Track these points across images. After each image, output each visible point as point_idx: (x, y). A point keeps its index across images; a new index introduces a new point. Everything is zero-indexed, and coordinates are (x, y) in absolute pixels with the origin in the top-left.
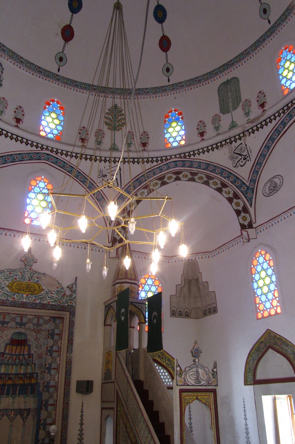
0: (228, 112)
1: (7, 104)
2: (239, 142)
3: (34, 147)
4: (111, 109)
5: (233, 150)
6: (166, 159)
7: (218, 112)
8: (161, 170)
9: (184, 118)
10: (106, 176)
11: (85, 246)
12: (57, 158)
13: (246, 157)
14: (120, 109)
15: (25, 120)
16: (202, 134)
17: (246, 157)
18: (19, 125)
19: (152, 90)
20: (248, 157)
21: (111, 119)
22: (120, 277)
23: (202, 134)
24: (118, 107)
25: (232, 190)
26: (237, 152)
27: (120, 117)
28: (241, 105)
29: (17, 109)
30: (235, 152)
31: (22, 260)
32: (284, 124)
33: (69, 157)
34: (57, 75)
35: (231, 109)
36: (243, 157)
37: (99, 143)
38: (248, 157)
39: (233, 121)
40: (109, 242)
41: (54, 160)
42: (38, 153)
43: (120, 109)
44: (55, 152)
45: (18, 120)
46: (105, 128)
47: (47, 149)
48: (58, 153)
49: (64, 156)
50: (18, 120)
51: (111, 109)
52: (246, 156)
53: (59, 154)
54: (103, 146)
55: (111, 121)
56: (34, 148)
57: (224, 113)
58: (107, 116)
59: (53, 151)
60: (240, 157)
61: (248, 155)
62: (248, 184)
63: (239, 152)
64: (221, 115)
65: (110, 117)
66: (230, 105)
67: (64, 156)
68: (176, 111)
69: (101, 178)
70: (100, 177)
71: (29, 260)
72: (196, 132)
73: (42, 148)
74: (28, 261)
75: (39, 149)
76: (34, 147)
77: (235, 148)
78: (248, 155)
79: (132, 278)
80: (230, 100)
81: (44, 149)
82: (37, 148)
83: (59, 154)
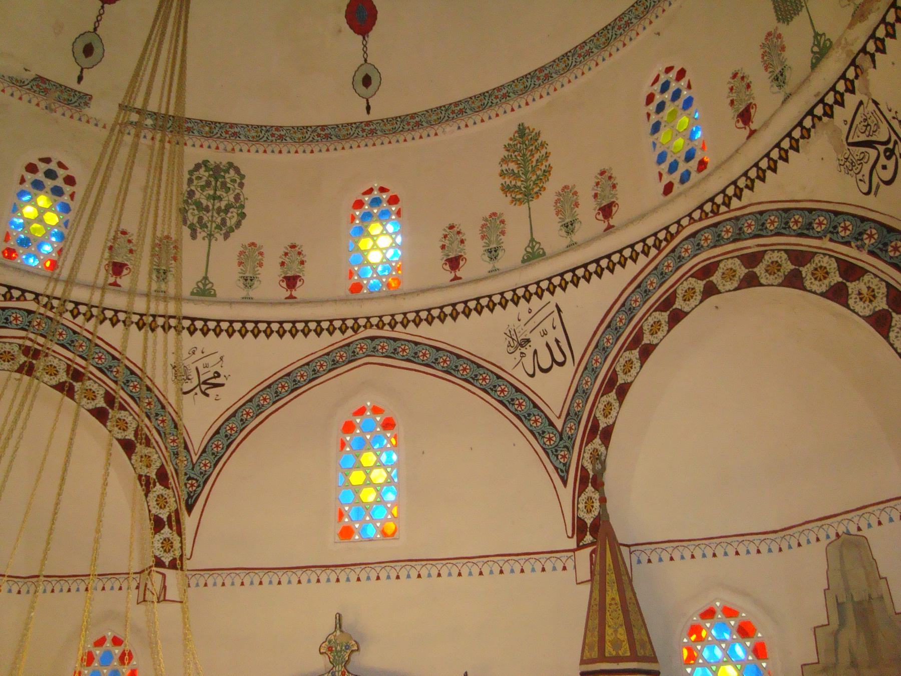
1: (261, 254)
2: (851, 101)
4: (511, 142)
5: (844, 137)
8: (663, 277)
9: (403, 213)
10: (528, 341)
11: (501, 563)
12: (395, 340)
13: (891, 146)
14: (533, 134)
17: (891, 146)
19: (598, 40)
20: (896, 143)
22: (587, 655)
24: (527, 131)
26: (856, 140)
27: (537, 156)
30: (850, 140)
31: (322, 651)
34: (368, 123)
36: (881, 148)
38: (896, 143)
39: (816, 35)
40: (568, 537)
41: (389, 347)
43: (533, 134)
47: (368, 325)
50: (291, 282)
51: (511, 142)
52: (888, 142)
53: (399, 327)
55: (516, 176)
60: (873, 153)
61: (894, 138)
63: (863, 138)
64: (783, 28)
69: (518, 352)
70: (512, 350)
71: (339, 648)
74: (337, 652)
75: (350, 332)
77: (848, 126)
78: (894, 138)
79: (621, 653)
81: (362, 329)
83: (399, 327)
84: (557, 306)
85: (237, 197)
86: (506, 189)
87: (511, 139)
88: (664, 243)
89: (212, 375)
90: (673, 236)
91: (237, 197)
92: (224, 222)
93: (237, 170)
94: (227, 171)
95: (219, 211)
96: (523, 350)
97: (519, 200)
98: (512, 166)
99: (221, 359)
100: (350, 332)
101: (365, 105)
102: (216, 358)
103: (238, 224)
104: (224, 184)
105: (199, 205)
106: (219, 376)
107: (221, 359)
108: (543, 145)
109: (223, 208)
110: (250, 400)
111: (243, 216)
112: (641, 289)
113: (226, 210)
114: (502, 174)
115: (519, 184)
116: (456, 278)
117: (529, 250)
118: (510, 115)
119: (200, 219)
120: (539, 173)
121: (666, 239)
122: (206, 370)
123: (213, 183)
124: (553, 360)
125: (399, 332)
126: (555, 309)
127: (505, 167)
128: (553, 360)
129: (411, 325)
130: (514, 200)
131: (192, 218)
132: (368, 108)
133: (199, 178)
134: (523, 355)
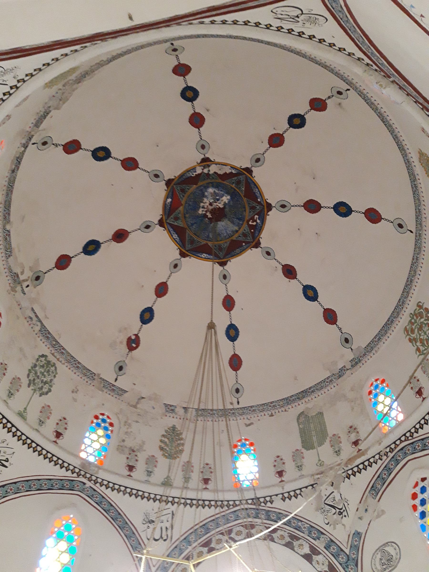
0: (312, 448)
1: (51, 413)
3: (70, 471)
6: (234, 505)
7: (299, 447)
8: (228, 521)
12: (95, 490)
13: (342, 511)
15: (67, 435)
16: (280, 473)
17: (342, 511)
18: (58, 441)
20: (344, 511)
21: (168, 443)
23: (280, 473)
25: (327, 559)
26: (328, 503)
28: (328, 441)
29: (61, 420)
30: (326, 502)
32: (388, 470)
33: (110, 489)
35: (316, 444)
36: (338, 510)
37: (149, 473)
38: (344, 511)
39: (320, 460)
41: (90, 492)
42: (72, 481)
44: (94, 481)
45: (58, 435)
46: (158, 454)
47: (85, 476)
48: (97, 482)
49: (103, 488)
50: (58, 435)
52: (341, 509)
53: (98, 485)
54: (153, 479)
56: (69, 473)
57: (307, 449)
58: (163, 439)
59: (92, 480)
60: (333, 511)
61: (344, 509)
62: (347, 551)
63: (331, 504)
64: (304, 450)
65: (166, 440)
66: (314, 439)
67: (103, 488)
68: (246, 440)
69: (147, 525)
72: (273, 471)
73: (79, 475)
75: (75, 475)
76: (70, 471)
77: (326, 497)
78: (344, 509)
80: (313, 433)
81: (81, 476)
82: (73, 473)
83: (98, 485)
84: (173, 512)
85: (51, 380)
86: (161, 449)
87: (169, 429)
88: (231, 507)
89: (4, 459)
90: (237, 506)
91: (51, 380)
92: (41, 388)
93: (56, 368)
94: (52, 366)
95: (42, 381)
96: (149, 525)
97: (166, 456)
98: (166, 440)
99: (14, 453)
100: (75, 475)
101: (116, 377)
102: (11, 451)
103: (47, 393)
104: (48, 371)
105: (36, 373)
106: (7, 461)
107: (14, 453)
108: (182, 439)
109: (44, 381)
110: (15, 483)
111: (50, 390)
112: (215, 521)
113: (46, 383)
114: (161, 441)
115: (168, 449)
116: (129, 476)
117: (166, 480)
118: (171, 419)
119: (34, 380)
120: (177, 449)
121: (233, 505)
122: (4, 454)
123: (45, 367)
124: (161, 537)
125: (97, 487)
126: (171, 513)
127: (163, 439)
128: (161, 537)
129: (104, 487)
130: (163, 455)
131: (31, 378)
132: (116, 380)
133: (41, 361)
134: (148, 527)
